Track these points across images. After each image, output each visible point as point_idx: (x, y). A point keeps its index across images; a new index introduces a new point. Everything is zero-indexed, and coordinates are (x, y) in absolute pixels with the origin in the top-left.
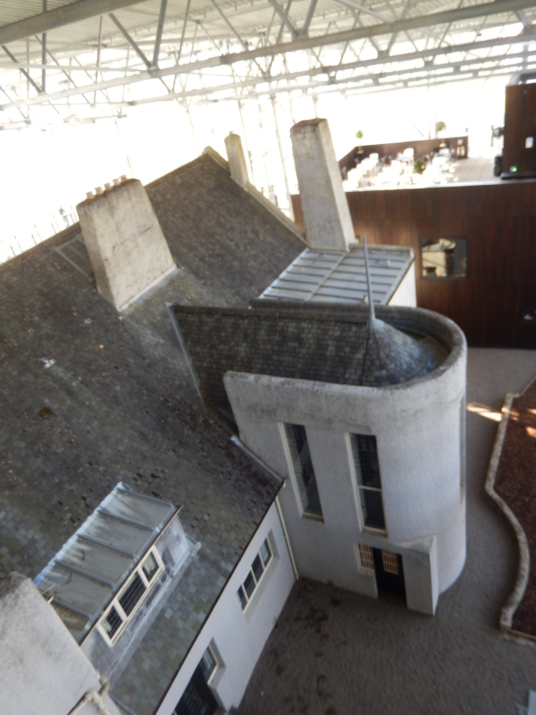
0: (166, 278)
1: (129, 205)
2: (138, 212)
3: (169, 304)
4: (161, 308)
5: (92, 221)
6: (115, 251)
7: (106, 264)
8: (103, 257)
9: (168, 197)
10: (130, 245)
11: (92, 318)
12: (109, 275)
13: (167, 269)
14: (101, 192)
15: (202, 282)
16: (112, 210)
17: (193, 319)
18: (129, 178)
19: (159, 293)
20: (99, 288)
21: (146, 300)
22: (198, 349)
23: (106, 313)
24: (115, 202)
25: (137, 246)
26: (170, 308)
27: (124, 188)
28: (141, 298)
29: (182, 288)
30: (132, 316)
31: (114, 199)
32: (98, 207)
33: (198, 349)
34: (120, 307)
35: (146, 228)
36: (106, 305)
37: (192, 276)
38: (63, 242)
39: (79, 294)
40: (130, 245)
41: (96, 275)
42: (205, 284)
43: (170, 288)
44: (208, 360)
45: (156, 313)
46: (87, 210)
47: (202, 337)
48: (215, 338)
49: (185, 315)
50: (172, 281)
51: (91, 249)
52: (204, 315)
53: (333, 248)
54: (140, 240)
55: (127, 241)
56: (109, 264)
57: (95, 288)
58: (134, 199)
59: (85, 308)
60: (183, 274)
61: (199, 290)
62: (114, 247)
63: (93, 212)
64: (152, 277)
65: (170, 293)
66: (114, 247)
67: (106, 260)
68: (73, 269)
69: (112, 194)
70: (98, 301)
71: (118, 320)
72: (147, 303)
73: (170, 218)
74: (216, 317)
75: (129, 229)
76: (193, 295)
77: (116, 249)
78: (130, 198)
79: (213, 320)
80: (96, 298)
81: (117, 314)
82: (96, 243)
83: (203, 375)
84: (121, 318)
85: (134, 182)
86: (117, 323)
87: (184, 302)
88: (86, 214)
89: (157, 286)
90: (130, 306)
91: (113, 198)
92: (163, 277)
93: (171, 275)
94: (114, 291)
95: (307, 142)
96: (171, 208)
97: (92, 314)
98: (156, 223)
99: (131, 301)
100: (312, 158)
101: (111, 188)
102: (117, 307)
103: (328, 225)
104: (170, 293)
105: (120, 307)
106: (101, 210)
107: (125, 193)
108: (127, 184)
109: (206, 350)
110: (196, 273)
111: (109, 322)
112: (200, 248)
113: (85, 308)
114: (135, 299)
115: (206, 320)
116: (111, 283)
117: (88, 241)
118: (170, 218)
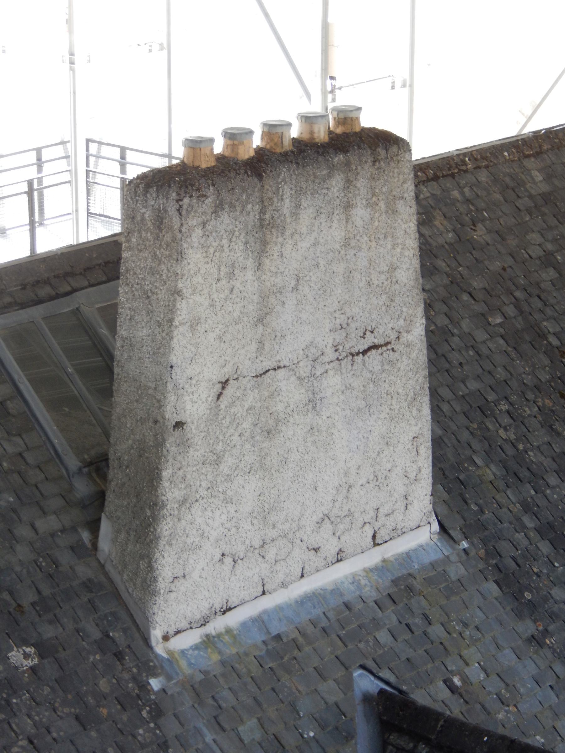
0: (384, 567)
1: (335, 233)
2: (359, 269)
3: (365, 683)
4: (330, 691)
5: (180, 256)
6: (224, 402)
7: (171, 445)
8: (171, 416)
9: (480, 234)
10: (290, 391)
11: (43, 649)
12: (171, 493)
13: (397, 533)
14: (246, 153)
15: (528, 627)
16: (265, 231)
18: (367, 121)
19: (338, 625)
20: (105, 527)
21: (278, 637)
23: (105, 644)
24: (287, 206)
25: (313, 403)
26: (367, 698)
27: (339, 158)
28: (259, 621)
29: (437, 631)
30: (202, 688)
31: (287, 191)
32: (218, 208)
34: (166, 638)
35: (370, 340)
36: (117, 609)
37: (492, 588)
38: (23, 306)
39: (23, 531)
40: (290, 391)
41: (116, 475)
42: (536, 641)
43: (390, 617)
45: (305, 706)
46: (172, 209)
50: (402, 587)
51: (130, 365)
54: (332, 382)
55: (281, 373)
56: (185, 444)
57: (94, 527)
58: (360, 214)
59: (28, 597)
60: (456, 571)
61: (508, 658)
62: (225, 384)
63: (193, 221)
64: (330, 548)
65: (383, 636)
66: (225, 384)
67: (179, 425)
68: (30, 422)
69: (284, 171)
70: (88, 585)
71: (144, 687)
72: (280, 654)
73: (466, 325)
75: (305, 329)
76: (475, 673)
77: (229, 391)
78: (348, 206)
80: (84, 571)
81: (149, 664)
82: (161, 348)
84: (155, 684)
85: (384, 144)
86: (135, 698)
87: (430, 695)
88: (160, 220)
89: (336, 591)
90: (209, 641)
91: (285, 186)
92: (374, 557)
93: (407, 557)
94: (166, 563)
96: (477, 283)
97: (49, 632)
98: (417, 332)
99: (218, 625)
101: (287, 145)
102: (156, 634)
104: (383, 636)
105: (166, 638)
106: (226, 220)
107: (337, 182)
108: (348, 147)
110: (512, 582)
111: (104, 685)
112: (553, 480)
113: (28, 597)
114: (233, 620)
116: (165, 528)
117: (133, 330)
118: (466, 325)
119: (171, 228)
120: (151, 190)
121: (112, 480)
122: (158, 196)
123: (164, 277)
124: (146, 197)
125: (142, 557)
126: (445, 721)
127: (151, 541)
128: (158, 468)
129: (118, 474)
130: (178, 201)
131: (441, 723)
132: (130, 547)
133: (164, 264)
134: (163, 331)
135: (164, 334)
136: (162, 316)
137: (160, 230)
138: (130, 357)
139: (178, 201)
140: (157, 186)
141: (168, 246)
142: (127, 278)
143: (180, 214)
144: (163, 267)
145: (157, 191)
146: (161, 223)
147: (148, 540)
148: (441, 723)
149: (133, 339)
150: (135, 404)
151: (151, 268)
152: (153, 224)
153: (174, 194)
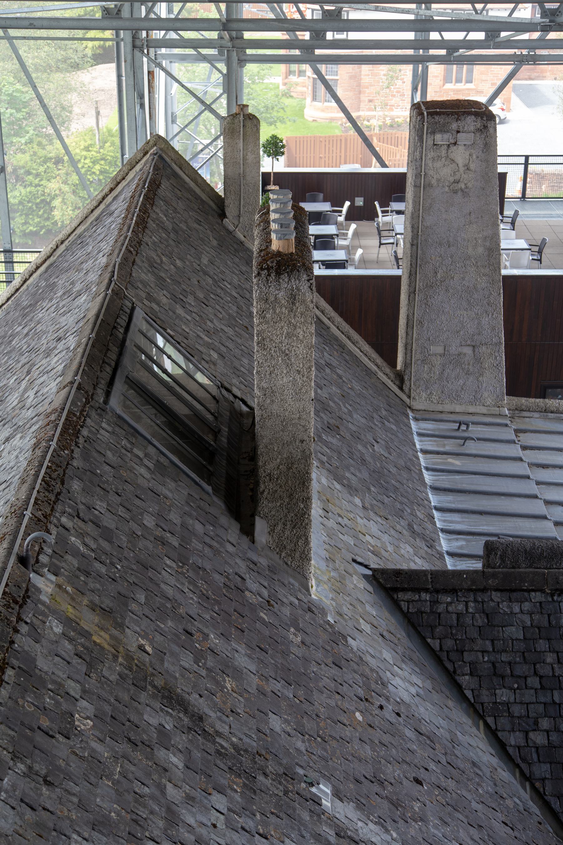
17: (461, 607)
22: (504, 695)
33: (504, 695)
44: (545, 724)
47: (505, 657)
48: (550, 658)
49: (426, 596)
52: (496, 596)
53: (471, 409)
74: (537, 597)
79: (527, 606)
83: (542, 770)
95: (460, 155)
100: (465, 193)
103: (468, 351)
109: (529, 696)
115: (504, 607)
119: (303, 302)
120: (282, 276)
121: (264, 491)
122: (290, 280)
123: (301, 337)
124: (279, 282)
125: (299, 538)
126: (431, 574)
127: (307, 524)
128: (307, 473)
129: (269, 485)
130: (308, 281)
131: (429, 576)
132: (287, 533)
133: (300, 328)
134: (303, 376)
135: (305, 379)
136: (301, 366)
137: (293, 303)
138: (273, 401)
139: (308, 281)
140: (287, 272)
141: (302, 314)
142: (264, 345)
143: (311, 289)
144: (299, 330)
145: (289, 276)
146: (295, 299)
147: (304, 524)
148: (429, 576)
149: (274, 388)
150: (281, 433)
151: (288, 333)
152: (287, 301)
153: (305, 276)
